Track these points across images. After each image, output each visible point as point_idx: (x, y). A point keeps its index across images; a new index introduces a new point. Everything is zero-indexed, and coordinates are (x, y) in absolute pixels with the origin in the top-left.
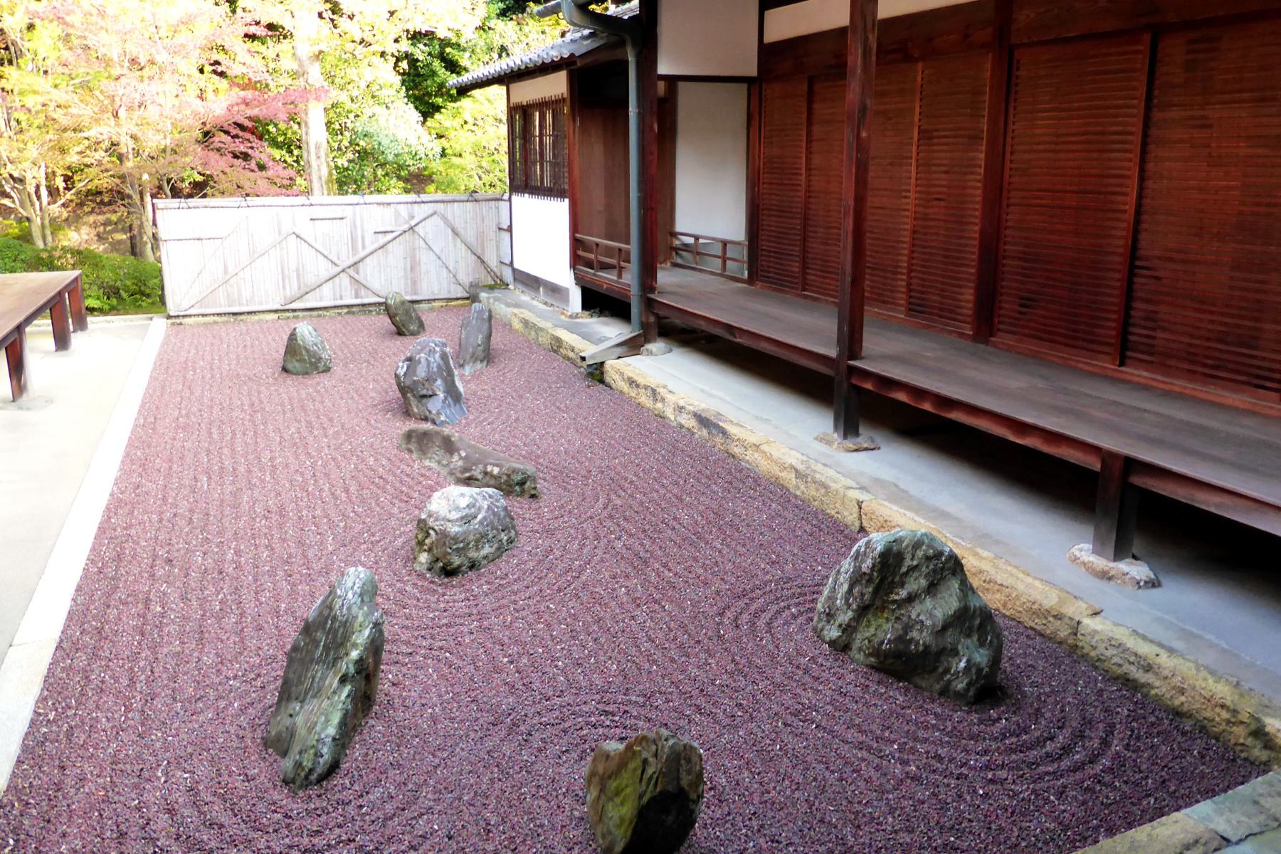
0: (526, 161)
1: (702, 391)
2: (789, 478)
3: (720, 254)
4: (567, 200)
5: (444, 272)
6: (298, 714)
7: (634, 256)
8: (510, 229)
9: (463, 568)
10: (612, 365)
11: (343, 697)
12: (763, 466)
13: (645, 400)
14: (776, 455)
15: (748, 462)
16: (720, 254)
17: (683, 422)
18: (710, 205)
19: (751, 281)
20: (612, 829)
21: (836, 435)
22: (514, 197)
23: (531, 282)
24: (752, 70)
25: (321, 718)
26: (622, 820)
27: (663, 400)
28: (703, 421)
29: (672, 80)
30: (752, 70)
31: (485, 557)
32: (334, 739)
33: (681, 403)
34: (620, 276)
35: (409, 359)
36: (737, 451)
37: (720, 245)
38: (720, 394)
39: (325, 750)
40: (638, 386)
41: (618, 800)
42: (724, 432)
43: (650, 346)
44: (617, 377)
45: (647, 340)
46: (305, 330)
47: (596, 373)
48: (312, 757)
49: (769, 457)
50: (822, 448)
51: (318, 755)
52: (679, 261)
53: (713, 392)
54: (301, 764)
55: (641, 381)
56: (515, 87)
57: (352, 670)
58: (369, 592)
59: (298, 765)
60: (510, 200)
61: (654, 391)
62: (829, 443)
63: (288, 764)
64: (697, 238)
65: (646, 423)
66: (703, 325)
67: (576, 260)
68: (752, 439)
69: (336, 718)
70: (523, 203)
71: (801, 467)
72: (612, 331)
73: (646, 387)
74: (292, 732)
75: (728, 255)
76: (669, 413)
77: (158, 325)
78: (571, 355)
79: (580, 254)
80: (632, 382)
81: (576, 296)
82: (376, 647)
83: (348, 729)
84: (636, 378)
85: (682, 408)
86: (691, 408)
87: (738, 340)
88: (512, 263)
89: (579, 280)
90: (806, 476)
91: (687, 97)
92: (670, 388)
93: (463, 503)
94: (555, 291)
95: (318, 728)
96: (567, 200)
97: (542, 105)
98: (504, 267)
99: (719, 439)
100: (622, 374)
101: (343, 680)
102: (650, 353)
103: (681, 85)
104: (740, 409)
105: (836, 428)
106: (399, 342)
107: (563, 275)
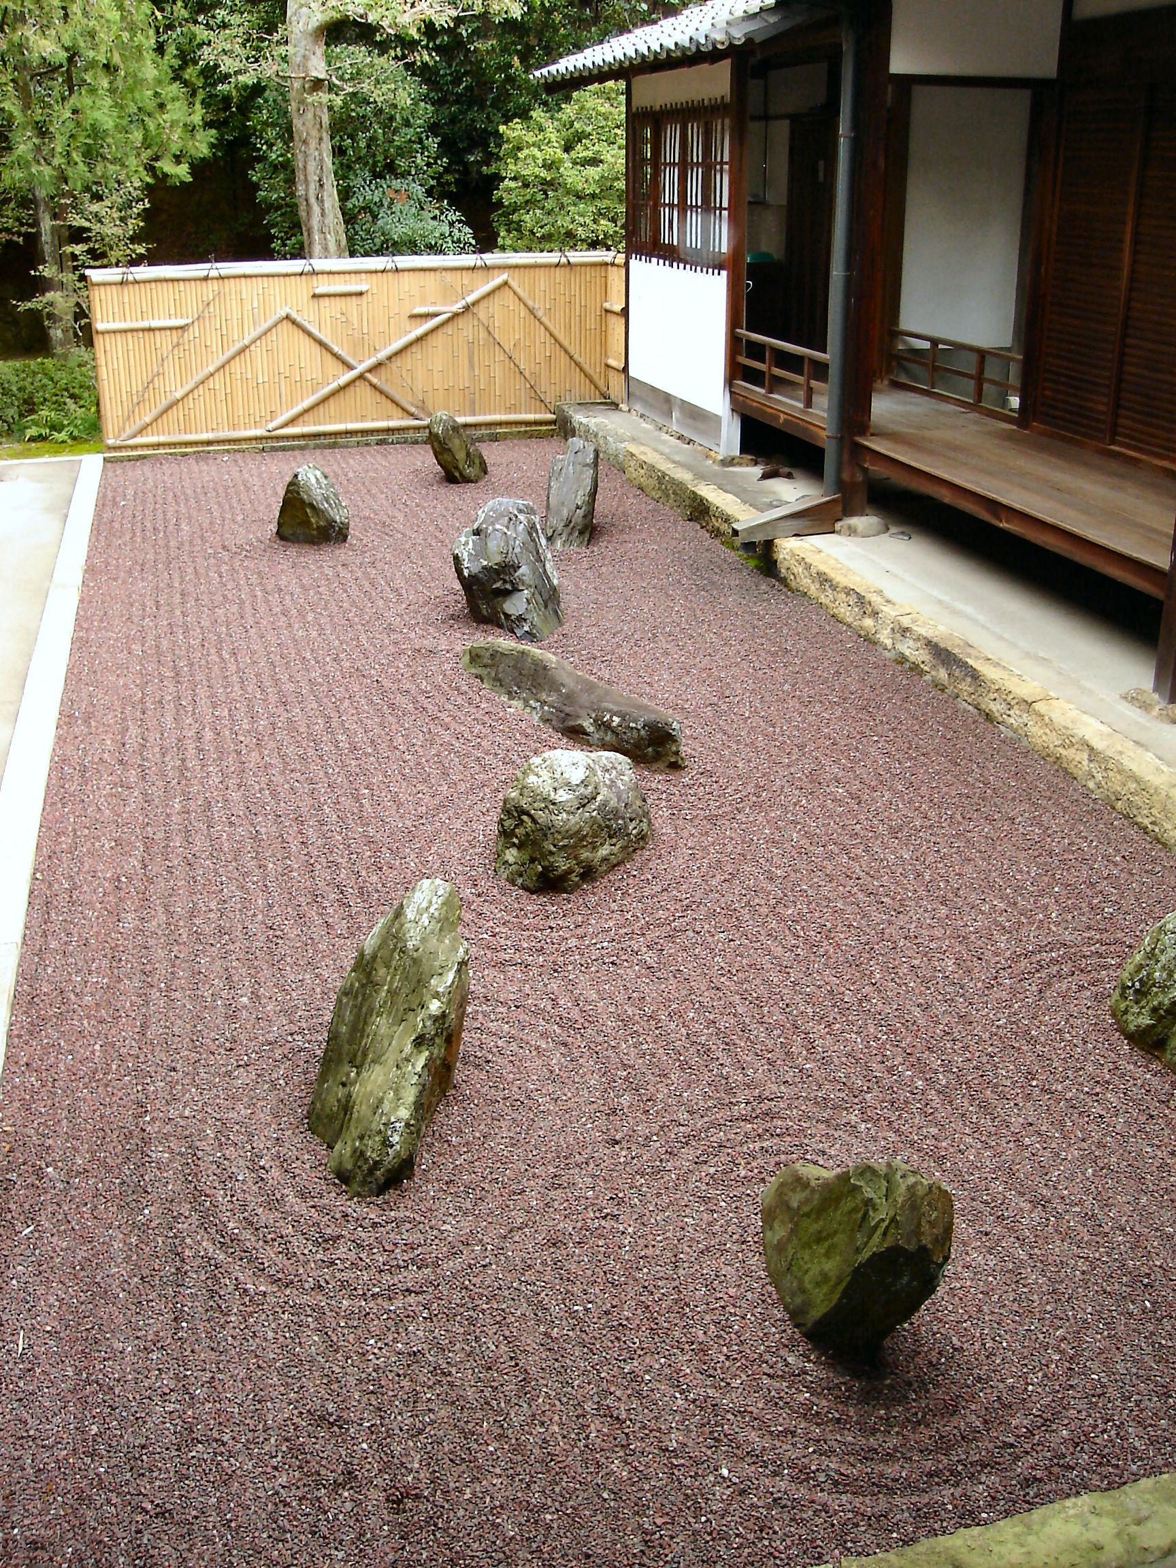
0: (635, 138)
1: (940, 602)
2: (1078, 759)
3: (973, 372)
4: (724, 273)
5: (519, 383)
6: (354, 1083)
7: (834, 372)
8: (625, 312)
9: (574, 878)
10: (789, 547)
11: (419, 1069)
12: (1038, 735)
13: (846, 612)
14: (1057, 716)
15: (1010, 727)
16: (973, 372)
17: (907, 653)
18: (960, 288)
19: (1024, 417)
20: (808, 1286)
21: (1156, 696)
22: (634, 263)
23: (663, 402)
24: (1045, 65)
25: (389, 1088)
26: (825, 1277)
27: (875, 614)
28: (942, 654)
29: (908, 82)
30: (1045, 65)
31: (605, 859)
32: (408, 1125)
33: (906, 621)
34: (809, 404)
35: (477, 532)
36: (996, 708)
37: (974, 358)
38: (969, 610)
39: (396, 1138)
40: (834, 588)
41: (821, 1249)
42: (975, 676)
43: (859, 522)
44: (799, 570)
45: (849, 511)
46: (311, 473)
47: (762, 557)
48: (378, 1146)
49: (1049, 724)
50: (1132, 713)
51: (386, 1143)
52: (903, 379)
53: (959, 606)
54: (362, 1153)
55: (838, 578)
56: (639, 82)
57: (431, 1029)
58: (448, 921)
59: (359, 1155)
60: (627, 264)
61: (860, 598)
62: (1146, 707)
63: (343, 1149)
64: (935, 342)
65: (843, 636)
66: (947, 497)
67: (736, 372)
68: (1023, 690)
69: (410, 1095)
70: (648, 274)
71: (1098, 744)
72: (793, 493)
73: (849, 591)
74: (346, 1106)
75: (987, 375)
76: (885, 638)
77: (91, 464)
78: (724, 527)
79: (742, 366)
80: (824, 580)
81: (730, 435)
82: (460, 997)
83: (425, 1109)
84: (832, 575)
85: (906, 630)
86: (922, 631)
87: (1003, 525)
88: (625, 369)
89: (738, 405)
90: (1106, 759)
91: (925, 110)
92: (888, 594)
93: (576, 776)
94: (695, 414)
95: (386, 1106)
96: (724, 273)
97: (685, 114)
98: (612, 373)
99: (965, 687)
100: (808, 567)
101: (419, 1042)
102: (852, 532)
103: (918, 91)
104: (1000, 638)
105: (1156, 689)
106: (455, 496)
107: (711, 394)
